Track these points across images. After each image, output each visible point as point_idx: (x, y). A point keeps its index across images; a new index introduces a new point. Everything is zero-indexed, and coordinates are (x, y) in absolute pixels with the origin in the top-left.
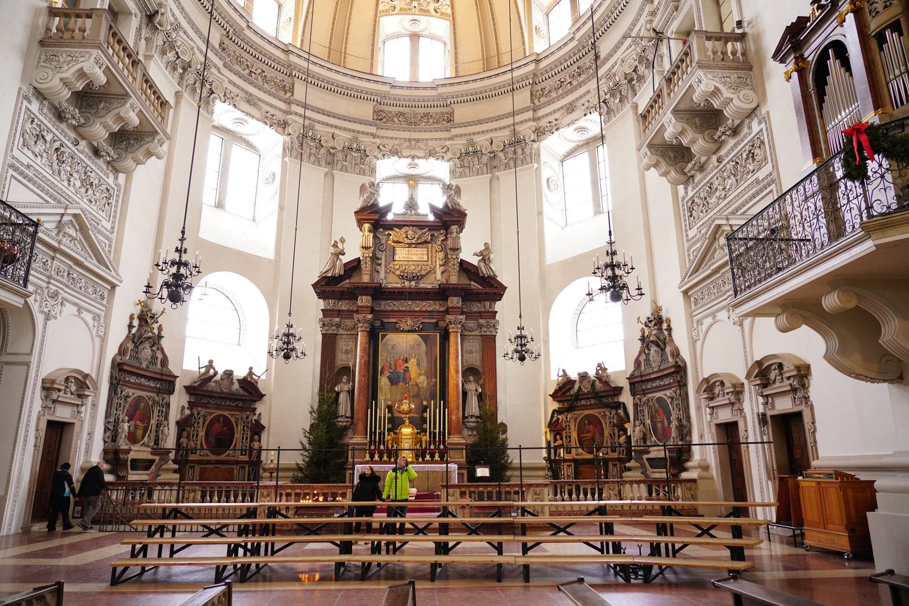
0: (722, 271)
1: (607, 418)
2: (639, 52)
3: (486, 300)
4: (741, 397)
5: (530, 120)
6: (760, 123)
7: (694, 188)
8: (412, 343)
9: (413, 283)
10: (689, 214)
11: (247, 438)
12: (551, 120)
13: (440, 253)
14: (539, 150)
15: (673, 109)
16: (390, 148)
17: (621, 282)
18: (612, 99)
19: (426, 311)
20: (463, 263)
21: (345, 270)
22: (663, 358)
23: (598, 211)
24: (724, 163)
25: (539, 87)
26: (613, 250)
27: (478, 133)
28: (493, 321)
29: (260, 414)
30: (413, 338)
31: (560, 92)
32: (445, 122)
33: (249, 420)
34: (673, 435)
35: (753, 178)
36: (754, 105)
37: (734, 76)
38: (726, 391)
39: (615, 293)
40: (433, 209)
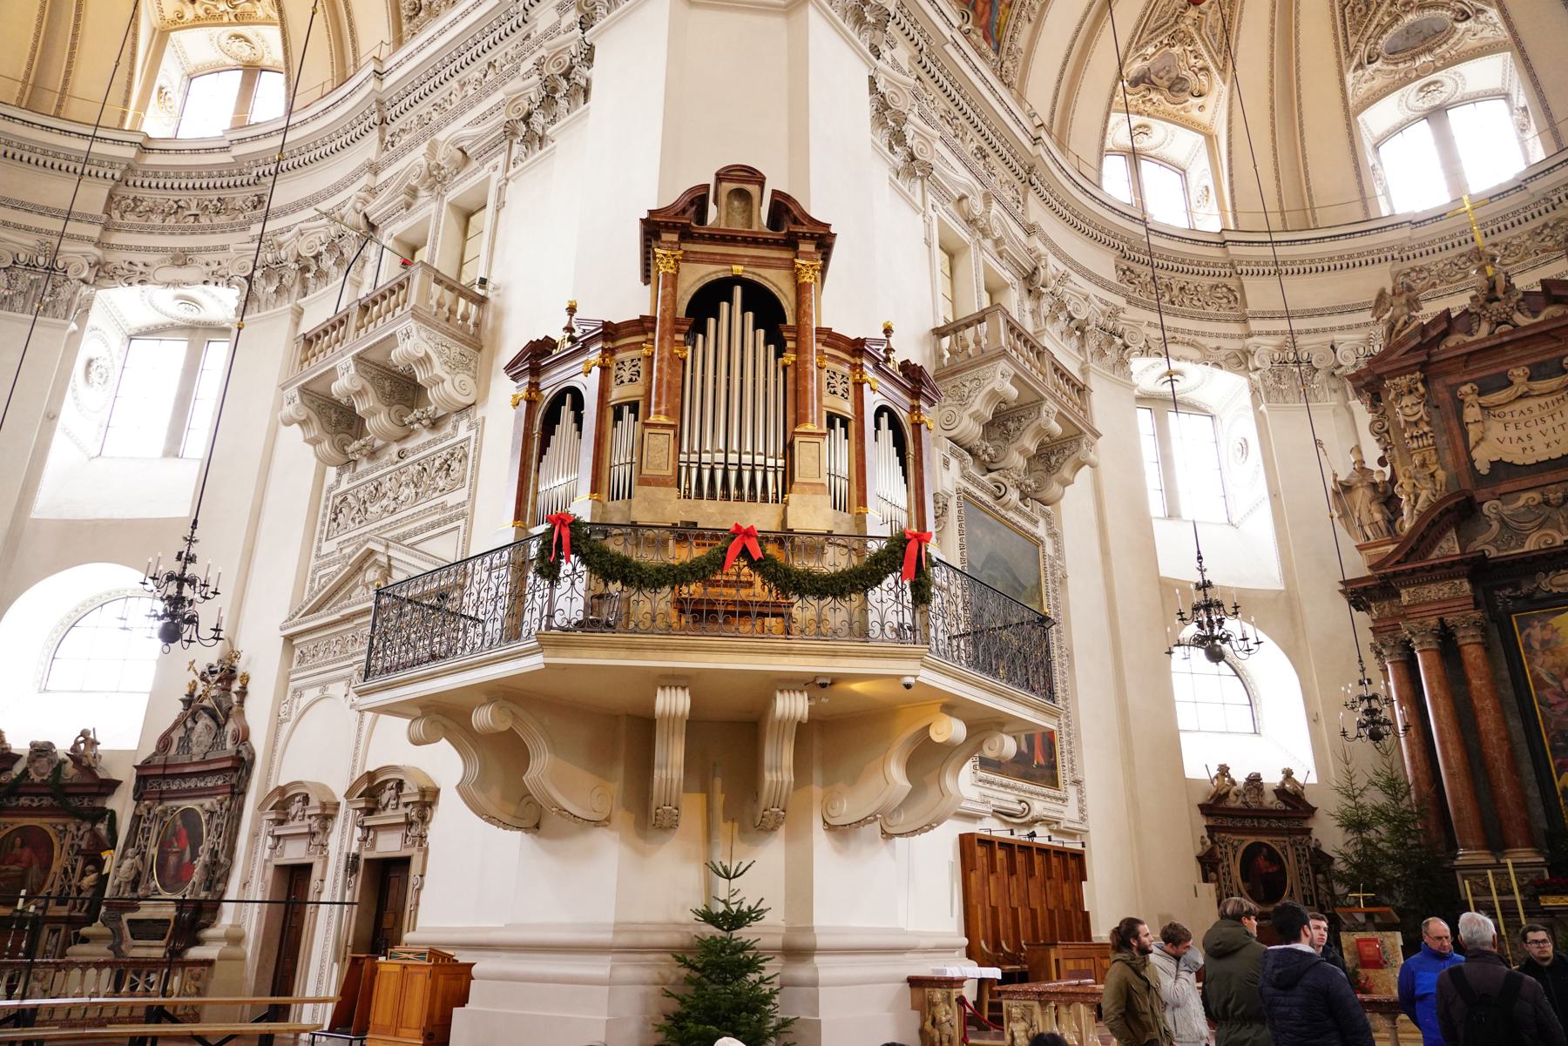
0: (356, 622)
1: (69, 837)
4: (330, 824)
5: (90, 240)
6: (470, 428)
7: (351, 480)
10: (333, 516)
12: (135, 261)
14: (90, 301)
15: (358, 355)
17: (187, 610)
18: (263, 282)
23: (173, 448)
24: (407, 461)
25: (132, 193)
26: (191, 552)
31: (171, 221)
34: (195, 878)
37: (456, 349)
38: (308, 812)
39: (172, 627)
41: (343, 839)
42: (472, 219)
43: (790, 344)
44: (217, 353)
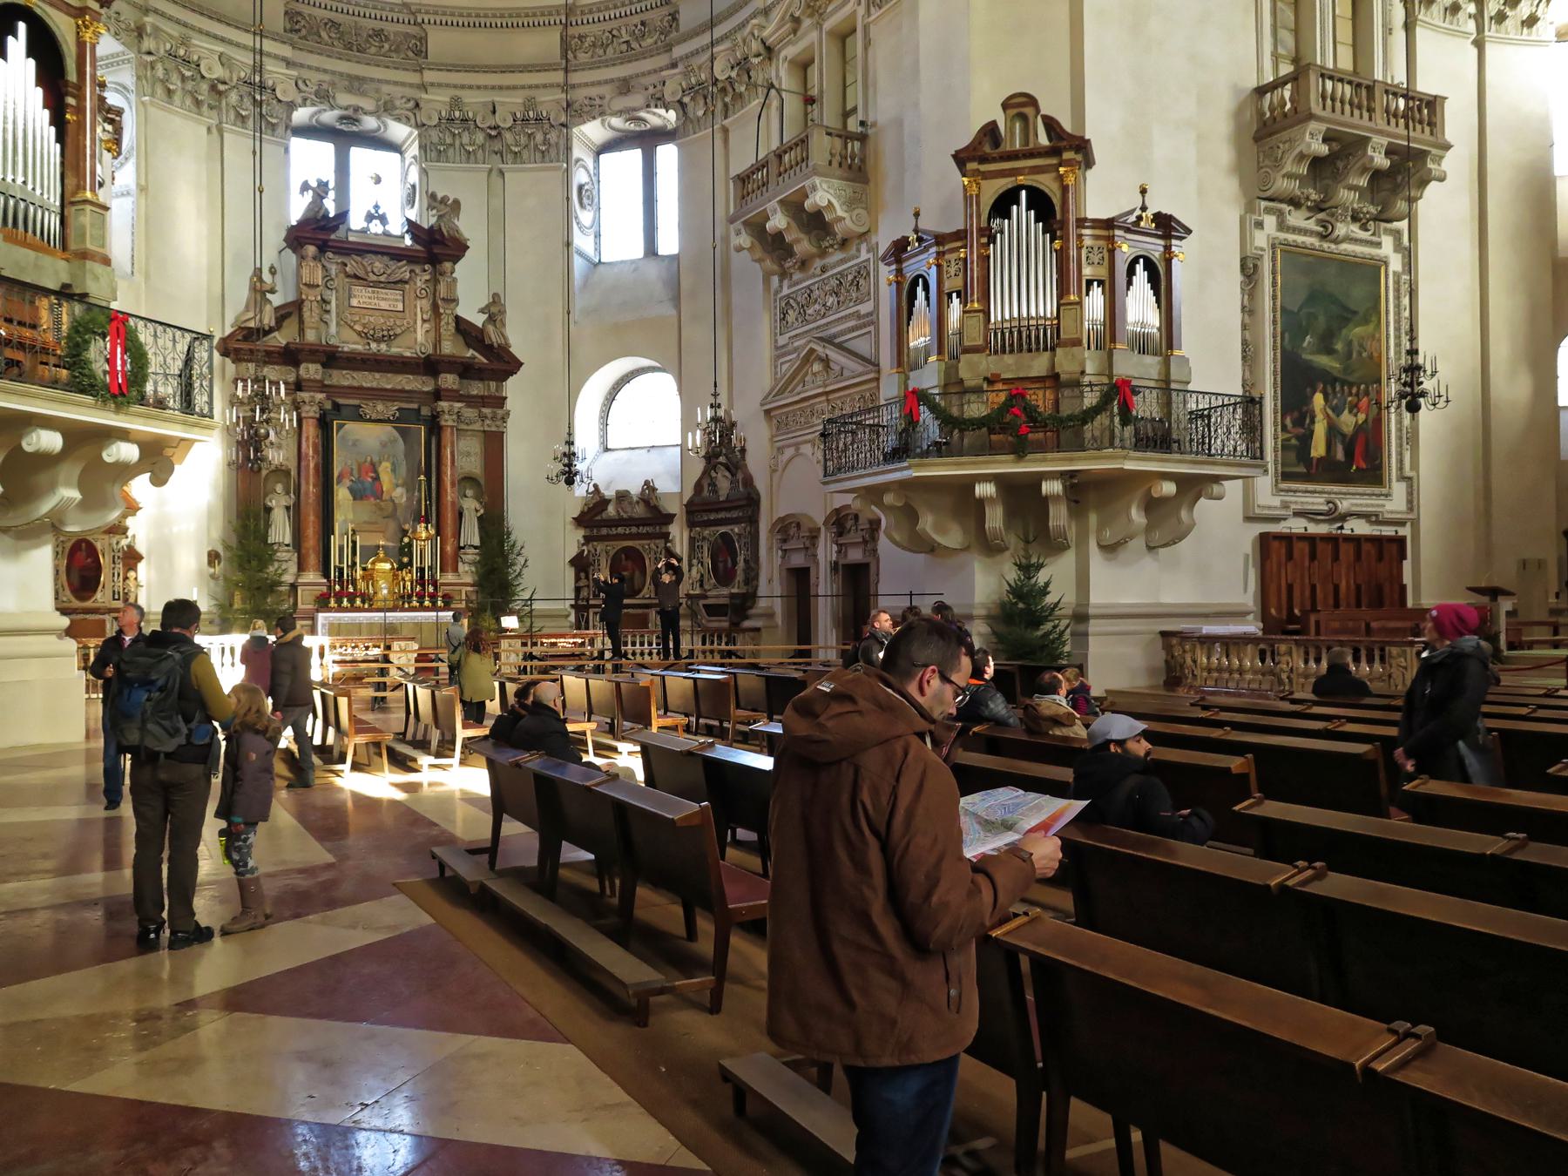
1: (652, 553)
2: (739, 57)
3: (492, 380)
6: (868, 251)
8: (384, 438)
9: (383, 347)
11: (119, 575)
13: (424, 301)
16: (315, 88)
19: (403, 391)
20: (458, 319)
21: (276, 318)
22: (734, 482)
27: (470, 87)
28: (500, 412)
29: (134, 536)
30: (386, 431)
32: (411, 54)
33: (120, 546)
35: (855, 309)
36: (862, 230)
38: (801, 535)
40: (413, 227)
41: (826, 551)
42: (848, 40)
43: (1058, 233)
44: (667, 155)
